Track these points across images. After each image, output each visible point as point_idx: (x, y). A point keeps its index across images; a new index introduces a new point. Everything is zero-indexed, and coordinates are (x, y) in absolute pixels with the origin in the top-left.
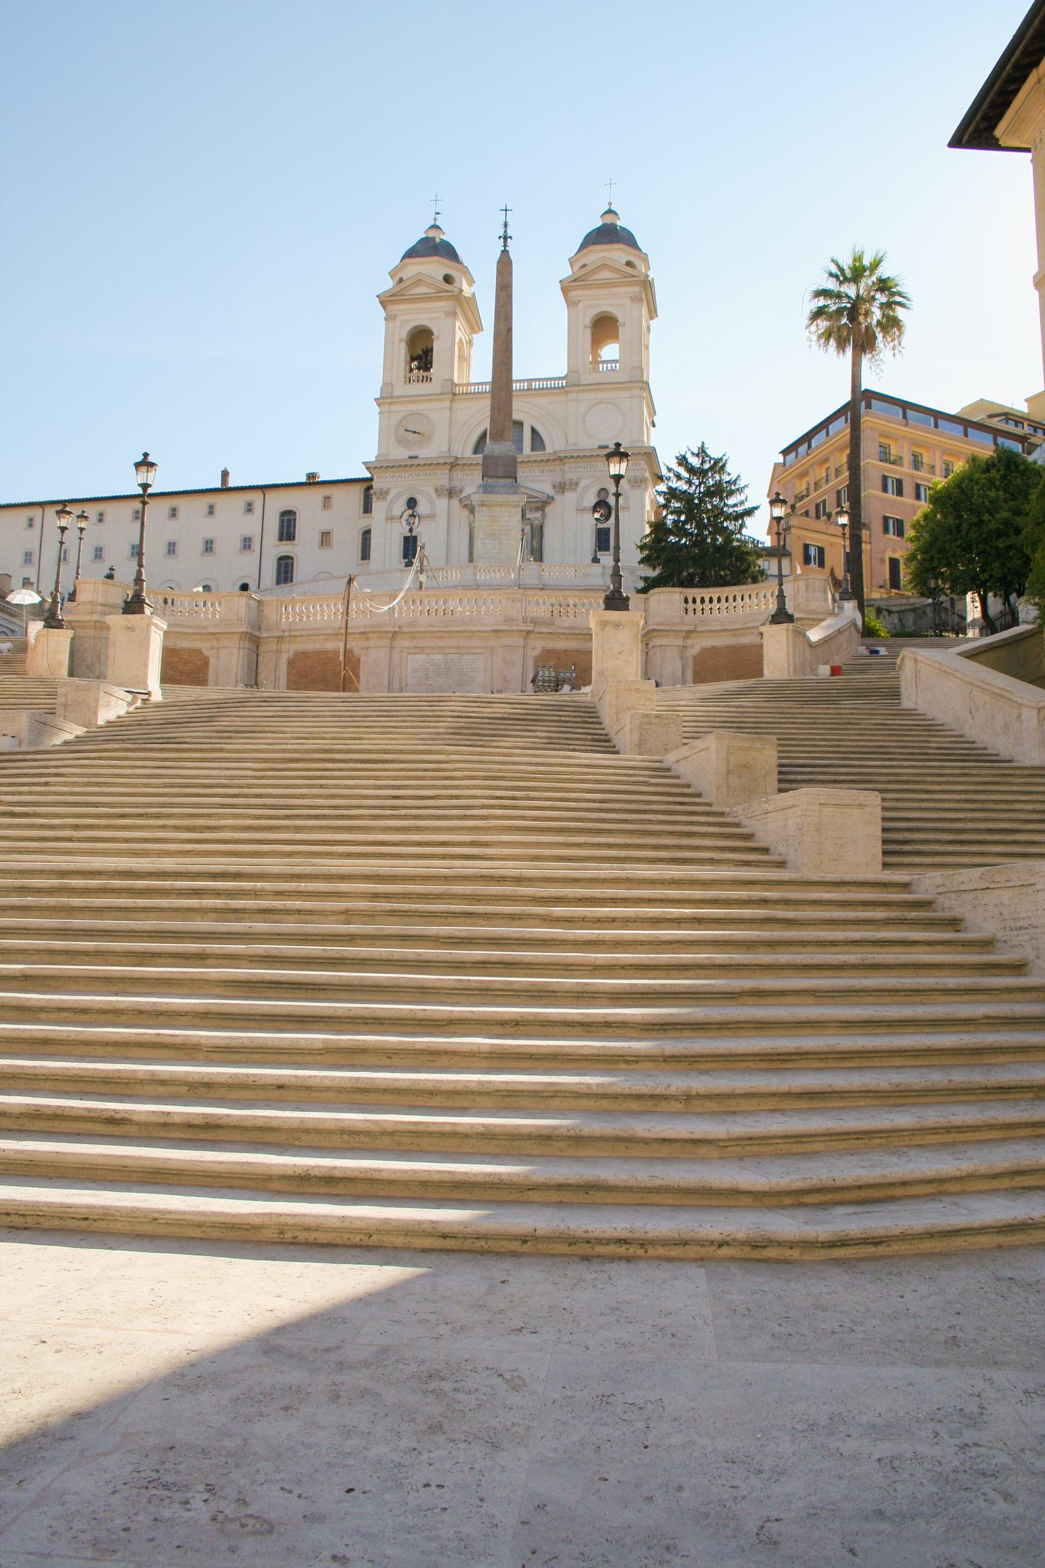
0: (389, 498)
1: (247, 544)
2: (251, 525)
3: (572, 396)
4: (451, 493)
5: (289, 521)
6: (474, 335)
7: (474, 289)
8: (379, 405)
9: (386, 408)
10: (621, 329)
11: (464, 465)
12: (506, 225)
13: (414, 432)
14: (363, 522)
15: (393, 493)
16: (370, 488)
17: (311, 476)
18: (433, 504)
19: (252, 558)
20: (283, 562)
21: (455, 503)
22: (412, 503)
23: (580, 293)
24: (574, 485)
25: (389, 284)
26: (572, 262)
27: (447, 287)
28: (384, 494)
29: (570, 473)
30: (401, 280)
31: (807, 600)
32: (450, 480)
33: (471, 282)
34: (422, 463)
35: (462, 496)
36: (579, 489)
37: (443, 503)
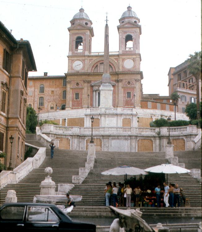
4: (89, 82)
6: (92, 38)
7: (92, 26)
8: (68, 57)
9: (70, 58)
12: (107, 17)
13: (78, 65)
17: (46, 74)
20: (41, 99)
21: (89, 85)
22: (78, 84)
24: (122, 81)
25: (69, 25)
26: (120, 20)
28: (70, 82)
29: (121, 77)
31: (192, 130)
33: (92, 24)
34: (80, 74)
37: (86, 84)
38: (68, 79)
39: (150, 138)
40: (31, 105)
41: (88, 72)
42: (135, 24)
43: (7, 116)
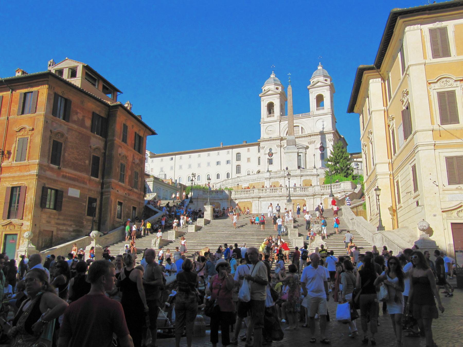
0: (265, 149)
1: (228, 162)
2: (229, 157)
3: (312, 118)
5: (239, 156)
10: (324, 98)
11: (284, 139)
13: (271, 131)
14: (259, 155)
15: (265, 148)
16: (259, 146)
18: (276, 150)
19: (229, 166)
20: (238, 166)
23: (312, 90)
27: (277, 91)
30: (265, 90)
32: (281, 144)
35: (284, 147)
36: (315, 143)
38: (262, 144)
39: (302, 198)
40: (229, 173)
41: (281, 136)
42: (326, 82)
43: (101, 181)
